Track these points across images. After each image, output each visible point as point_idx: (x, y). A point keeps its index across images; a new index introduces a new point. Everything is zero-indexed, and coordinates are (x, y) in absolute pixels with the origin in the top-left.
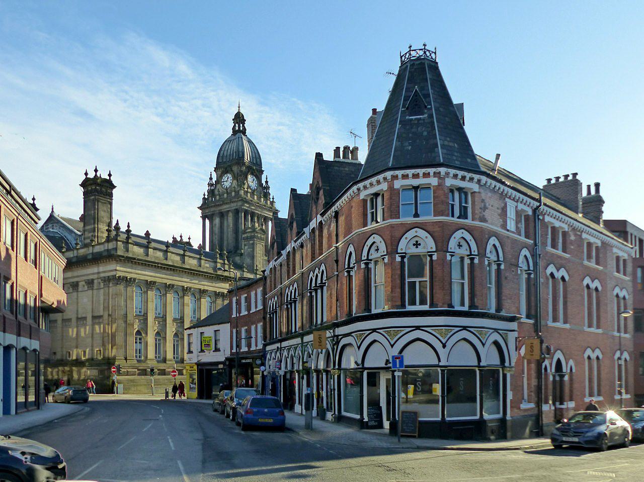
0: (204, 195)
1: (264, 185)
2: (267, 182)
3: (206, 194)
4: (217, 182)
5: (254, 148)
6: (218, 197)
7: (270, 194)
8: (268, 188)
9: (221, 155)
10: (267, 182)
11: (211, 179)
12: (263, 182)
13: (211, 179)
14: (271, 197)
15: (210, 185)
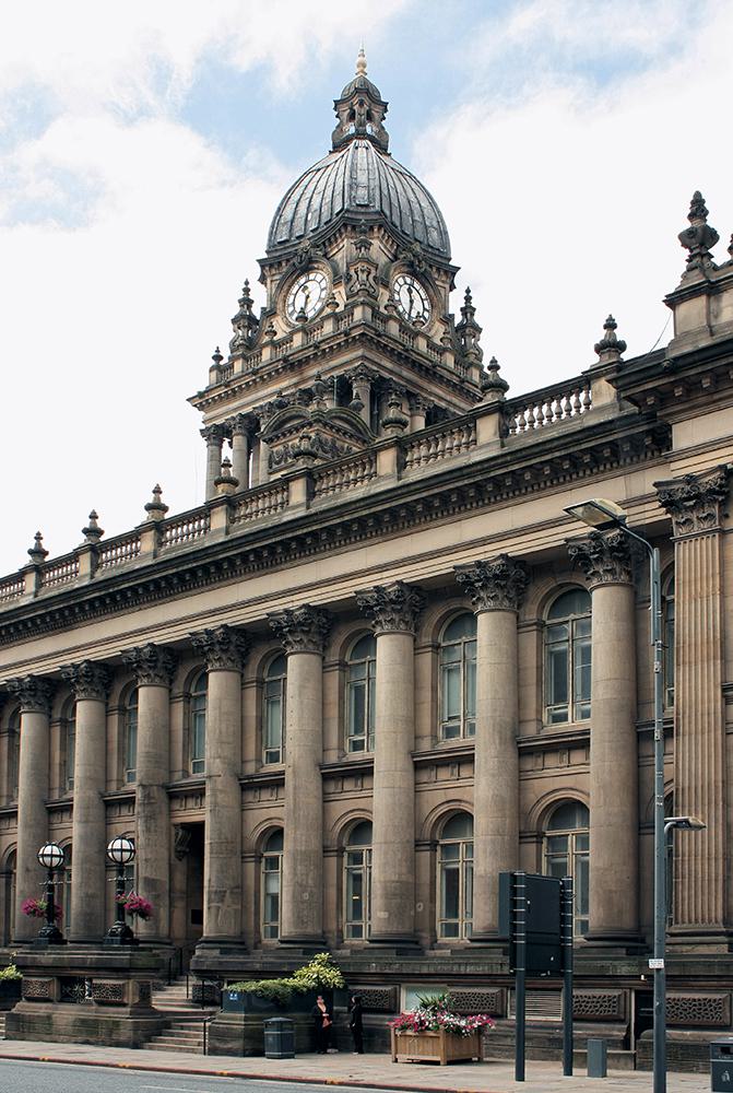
0: (218, 358)
1: (458, 319)
2: (468, 310)
3: (226, 353)
4: (269, 313)
5: (421, 196)
6: (266, 354)
7: (479, 355)
8: (469, 328)
9: (288, 213)
10: (468, 310)
11: (247, 302)
12: (455, 303)
13: (247, 302)
14: (486, 362)
15: (245, 320)
